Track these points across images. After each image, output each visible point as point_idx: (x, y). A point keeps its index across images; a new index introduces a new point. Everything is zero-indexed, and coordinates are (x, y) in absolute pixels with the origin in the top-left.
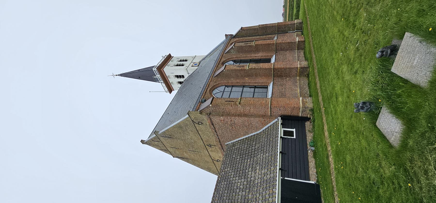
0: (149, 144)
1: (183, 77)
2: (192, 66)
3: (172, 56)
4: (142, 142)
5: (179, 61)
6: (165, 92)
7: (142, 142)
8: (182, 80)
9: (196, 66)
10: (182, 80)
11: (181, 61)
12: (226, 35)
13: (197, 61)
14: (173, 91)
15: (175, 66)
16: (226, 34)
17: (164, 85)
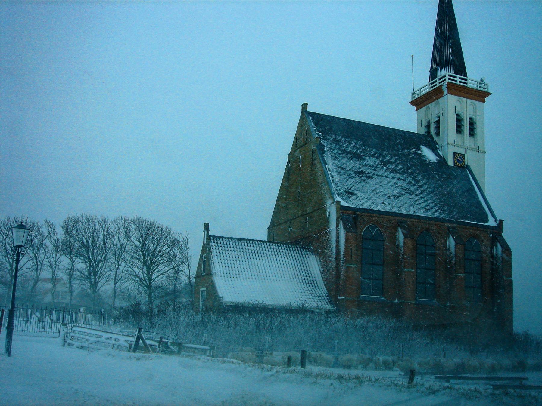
0: (302, 118)
1: (438, 134)
2: (455, 154)
3: (486, 99)
4: (305, 106)
5: (470, 119)
6: (412, 91)
7: (305, 106)
8: (433, 131)
9: (456, 162)
10: (433, 131)
11: (472, 124)
12: (504, 220)
13: (470, 160)
14: (414, 108)
15: (458, 115)
16: (504, 223)
17: (425, 91)
